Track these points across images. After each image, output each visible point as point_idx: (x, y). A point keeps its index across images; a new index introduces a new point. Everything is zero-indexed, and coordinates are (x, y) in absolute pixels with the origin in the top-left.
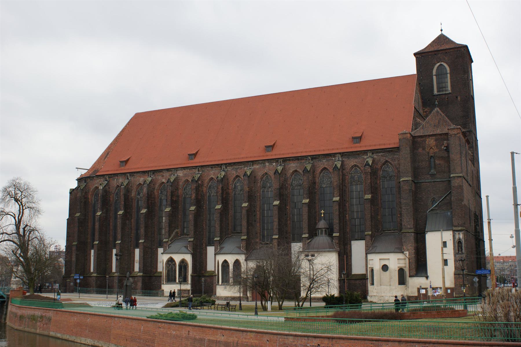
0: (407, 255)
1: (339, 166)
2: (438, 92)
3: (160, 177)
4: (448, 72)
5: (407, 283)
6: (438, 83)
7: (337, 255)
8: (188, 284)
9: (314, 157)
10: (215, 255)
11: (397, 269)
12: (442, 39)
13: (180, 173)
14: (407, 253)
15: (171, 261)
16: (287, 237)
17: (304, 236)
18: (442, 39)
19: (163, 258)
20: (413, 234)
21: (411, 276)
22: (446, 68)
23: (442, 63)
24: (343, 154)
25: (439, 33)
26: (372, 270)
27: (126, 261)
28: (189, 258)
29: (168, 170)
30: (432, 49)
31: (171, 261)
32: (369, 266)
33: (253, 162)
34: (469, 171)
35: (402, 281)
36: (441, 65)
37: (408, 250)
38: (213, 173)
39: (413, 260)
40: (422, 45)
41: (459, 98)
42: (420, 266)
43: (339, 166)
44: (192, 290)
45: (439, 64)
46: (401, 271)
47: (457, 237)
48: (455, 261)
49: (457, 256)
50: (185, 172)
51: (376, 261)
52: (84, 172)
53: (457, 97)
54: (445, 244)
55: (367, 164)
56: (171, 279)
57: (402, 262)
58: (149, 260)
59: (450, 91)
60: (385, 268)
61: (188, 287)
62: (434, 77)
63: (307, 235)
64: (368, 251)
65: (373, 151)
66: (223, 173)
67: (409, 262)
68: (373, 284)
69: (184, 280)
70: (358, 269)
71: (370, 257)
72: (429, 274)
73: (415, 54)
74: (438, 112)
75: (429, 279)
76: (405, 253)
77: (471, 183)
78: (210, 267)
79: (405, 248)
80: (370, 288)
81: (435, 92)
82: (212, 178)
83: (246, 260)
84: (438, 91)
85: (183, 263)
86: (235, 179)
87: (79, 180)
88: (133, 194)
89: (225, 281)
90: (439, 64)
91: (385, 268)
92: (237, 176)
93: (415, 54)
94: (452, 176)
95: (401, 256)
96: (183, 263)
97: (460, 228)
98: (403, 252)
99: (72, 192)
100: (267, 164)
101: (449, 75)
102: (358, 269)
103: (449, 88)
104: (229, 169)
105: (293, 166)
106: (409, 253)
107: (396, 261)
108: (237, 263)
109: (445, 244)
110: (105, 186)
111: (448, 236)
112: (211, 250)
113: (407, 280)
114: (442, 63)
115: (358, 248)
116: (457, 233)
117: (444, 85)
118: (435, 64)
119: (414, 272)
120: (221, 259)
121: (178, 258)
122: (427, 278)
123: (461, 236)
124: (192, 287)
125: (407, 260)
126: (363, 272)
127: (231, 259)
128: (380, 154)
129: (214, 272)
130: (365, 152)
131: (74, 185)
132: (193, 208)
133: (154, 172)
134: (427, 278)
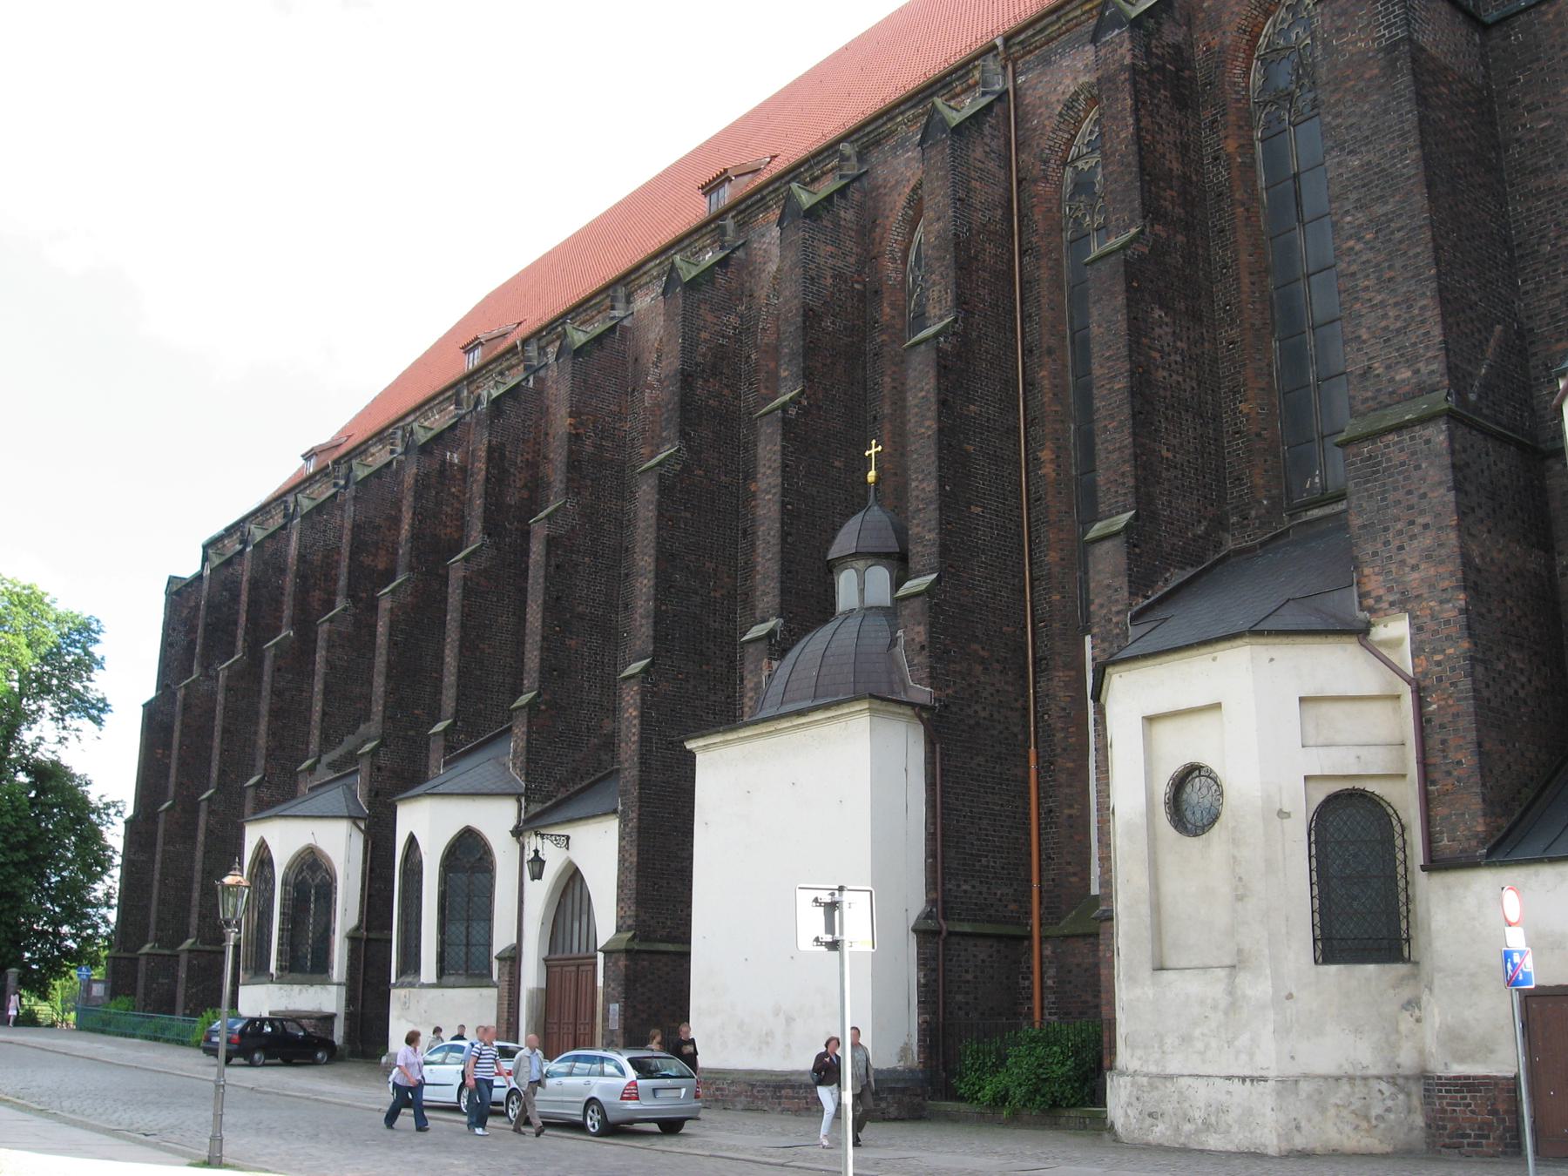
0: (1405, 659)
5: (1419, 940)
7: (905, 746)
8: (326, 981)
14: (1395, 629)
20: (1438, 434)
21: (1435, 864)
37: (1403, 603)
39: (1457, 701)
44: (349, 1017)
69: (305, 961)
76: (1381, 632)
79: (1374, 583)
95: (1333, 665)
96: (311, 865)
98: (1360, 633)
106: (1417, 629)
113: (1419, 907)
119: (1469, 819)
124: (351, 1000)
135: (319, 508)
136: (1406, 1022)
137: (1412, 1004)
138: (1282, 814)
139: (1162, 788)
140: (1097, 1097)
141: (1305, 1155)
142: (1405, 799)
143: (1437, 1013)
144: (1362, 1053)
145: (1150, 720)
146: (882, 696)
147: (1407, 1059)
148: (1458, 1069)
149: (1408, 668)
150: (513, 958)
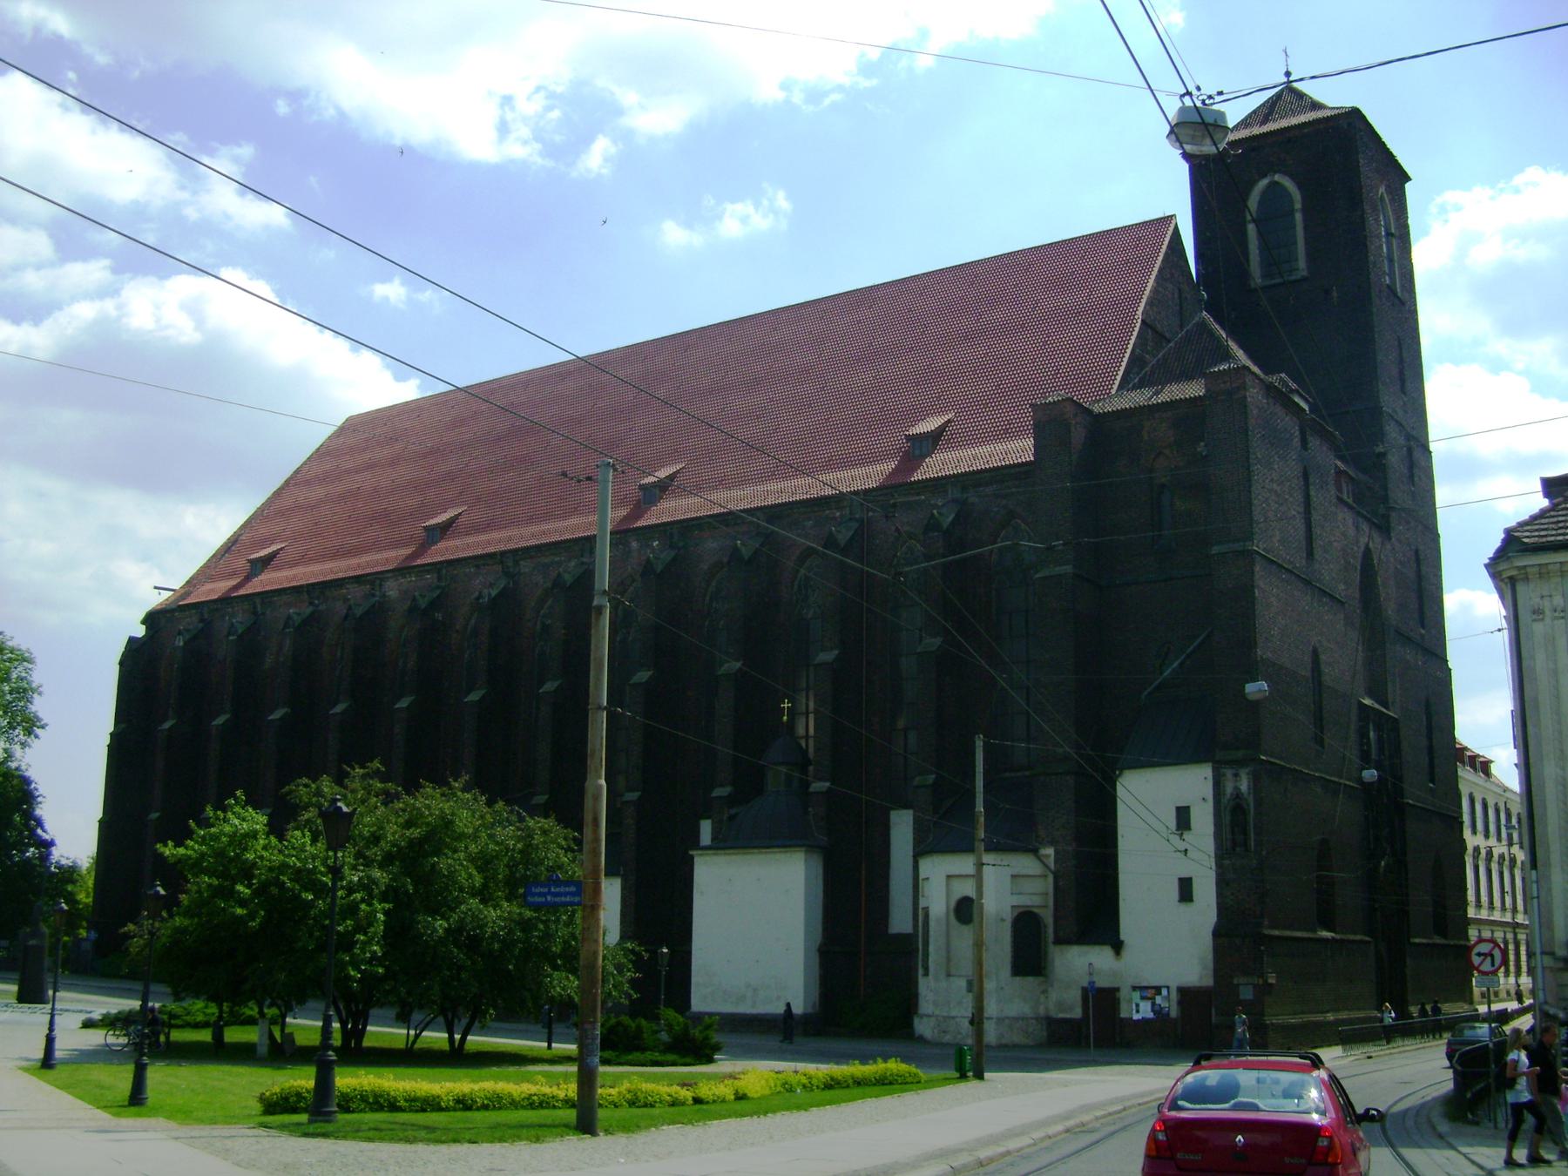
0: (1051, 862)
2: (1264, 276)
4: (1298, 206)
6: (1265, 247)
14: (1049, 851)
17: (719, 792)
21: (1059, 941)
22: (1289, 195)
23: (1277, 177)
26: (927, 916)
36: (1274, 184)
37: (1052, 843)
41: (1335, 294)
42: (1091, 906)
45: (1264, 183)
46: (1025, 925)
47: (1229, 789)
48: (1222, 883)
49: (1227, 862)
53: (1327, 292)
54: (1183, 818)
59: (1305, 273)
60: (965, 910)
62: (1251, 229)
64: (924, 847)
67: (1056, 888)
68: (926, 974)
72: (1125, 933)
75: (1125, 953)
80: (922, 981)
88: (269, 661)
90: (1264, 183)
91: (965, 910)
94: (1215, 550)
95: (1025, 864)
97: (1240, 754)
98: (1035, 851)
100: (634, 545)
101: (1298, 217)
103: (1302, 263)
106: (1057, 853)
107: (1007, 883)
109: (1183, 818)
110: (195, 638)
111: (1191, 784)
114: (1277, 177)
116: (1229, 773)
118: (1253, 183)
122: (1118, 947)
123: (1244, 786)
125: (1051, 879)
128: (989, 490)
135: (305, 622)
136: (1042, 998)
137: (1045, 992)
138: (1003, 920)
139: (953, 904)
140: (910, 1025)
141: (1006, 1046)
142: (1048, 917)
143: (1054, 995)
144: (1027, 1010)
145: (949, 877)
146: (810, 847)
147: (1042, 1011)
148: (1061, 1016)
149: (1052, 866)
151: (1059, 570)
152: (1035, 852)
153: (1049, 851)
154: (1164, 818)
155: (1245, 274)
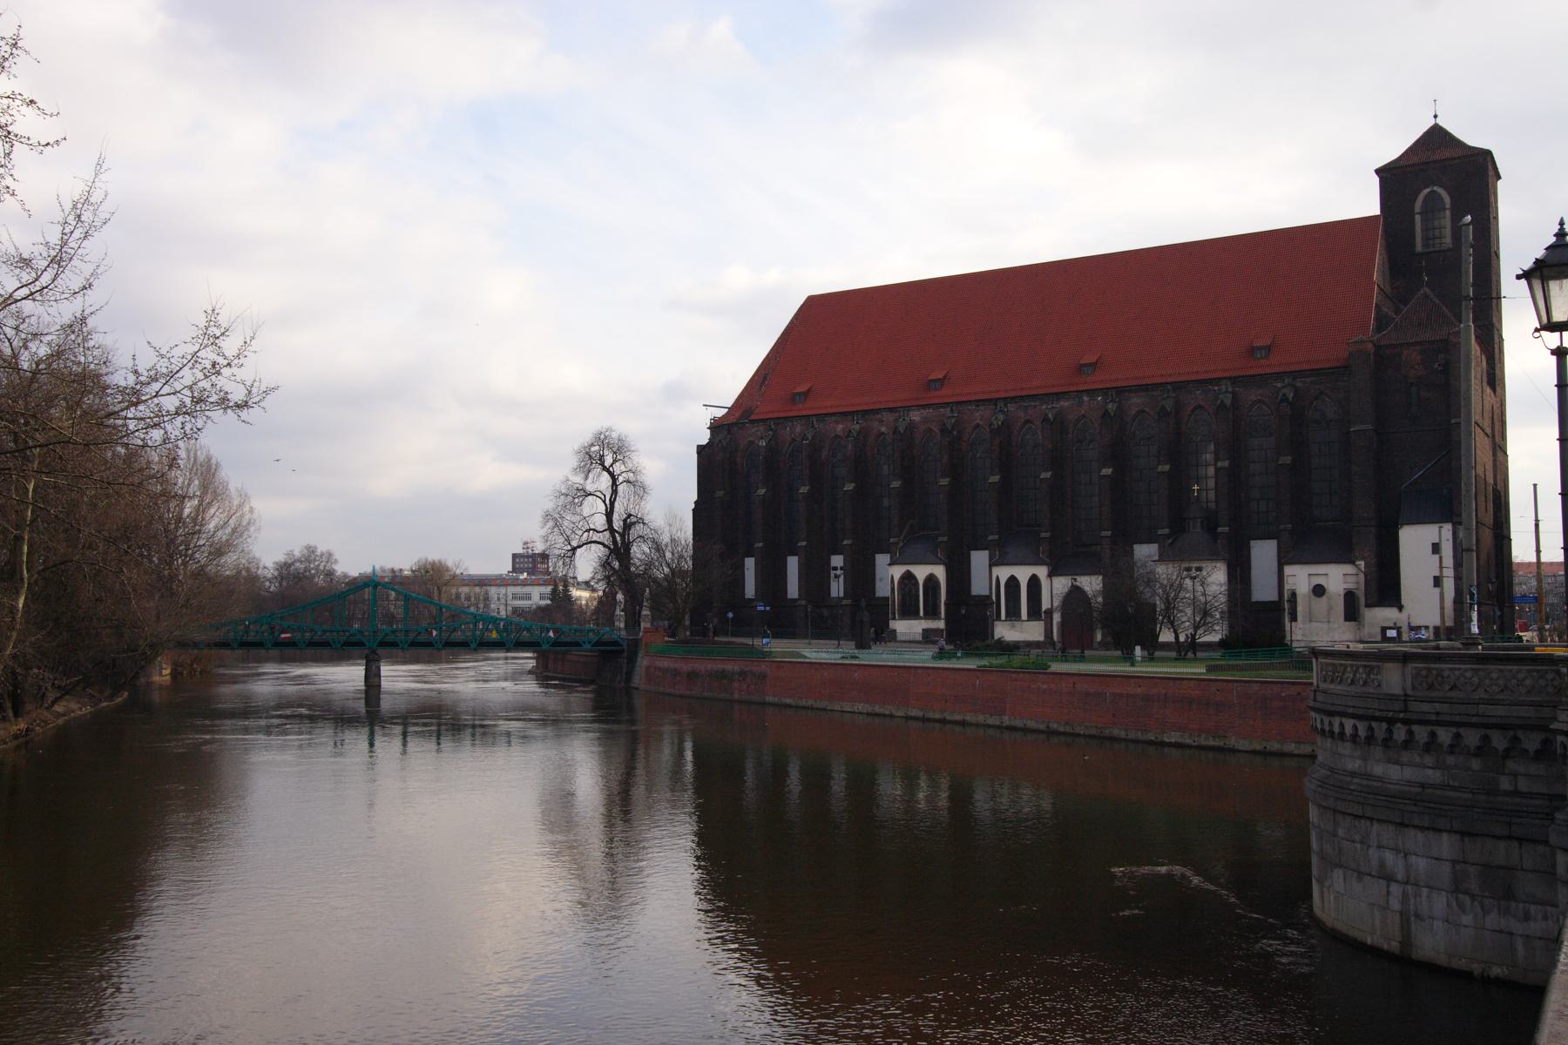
1: (1228, 402)
3: (876, 424)
6: (1425, 230)
9: (1178, 386)
10: (990, 566)
11: (1342, 593)
12: (1436, 137)
13: (915, 416)
14: (1362, 563)
15: (908, 577)
16: (1126, 536)
18: (1436, 137)
19: (889, 573)
21: (1367, 606)
24: (1234, 380)
25: (1431, 122)
26: (1294, 594)
27: (815, 576)
28: (940, 572)
29: (891, 410)
30: (1415, 160)
31: (908, 577)
32: (1287, 587)
33: (1058, 396)
34: (1487, 407)
35: (1352, 612)
38: (978, 416)
40: (1393, 149)
42: (1385, 585)
43: (1228, 402)
46: (1350, 596)
50: (925, 412)
51: (1300, 578)
52: (720, 413)
54: (1436, 548)
55: (1285, 399)
56: (909, 612)
57: (1353, 579)
58: (862, 576)
60: (1319, 591)
61: (941, 624)
62: (1418, 218)
63: (1167, 531)
65: (1295, 374)
66: (1001, 417)
68: (1294, 618)
69: (932, 613)
70: (1263, 589)
71: (1288, 570)
73: (1378, 171)
74: (1426, 296)
77: (1489, 431)
78: (979, 587)
81: (1419, 248)
82: (978, 426)
83: (1050, 575)
84: (1425, 245)
85: (931, 579)
86: (1022, 427)
87: (716, 426)
88: (824, 454)
89: (1013, 613)
91: (1319, 591)
92: (1027, 422)
93: (1378, 171)
95: (1349, 569)
96: (931, 579)
99: (701, 450)
101: (1448, 213)
102: (1263, 589)
104: (1011, 407)
105: (1136, 401)
107: (1338, 577)
108: (1034, 582)
109: (1436, 548)
112: (979, 559)
115: (1263, 553)
117: (1437, 233)
120: (1003, 573)
121: (921, 572)
122: (1400, 608)
125: (1362, 576)
126: (1271, 596)
127: (1023, 574)
129: (989, 597)
130: (1279, 376)
131: (704, 437)
132: (945, 482)
133: (865, 413)
134: (1400, 608)
143: (1366, 630)
150: (1049, 612)
151: (1362, 427)
152: (1352, 562)
153: (1362, 563)
154: (1422, 550)
155: (1413, 245)
